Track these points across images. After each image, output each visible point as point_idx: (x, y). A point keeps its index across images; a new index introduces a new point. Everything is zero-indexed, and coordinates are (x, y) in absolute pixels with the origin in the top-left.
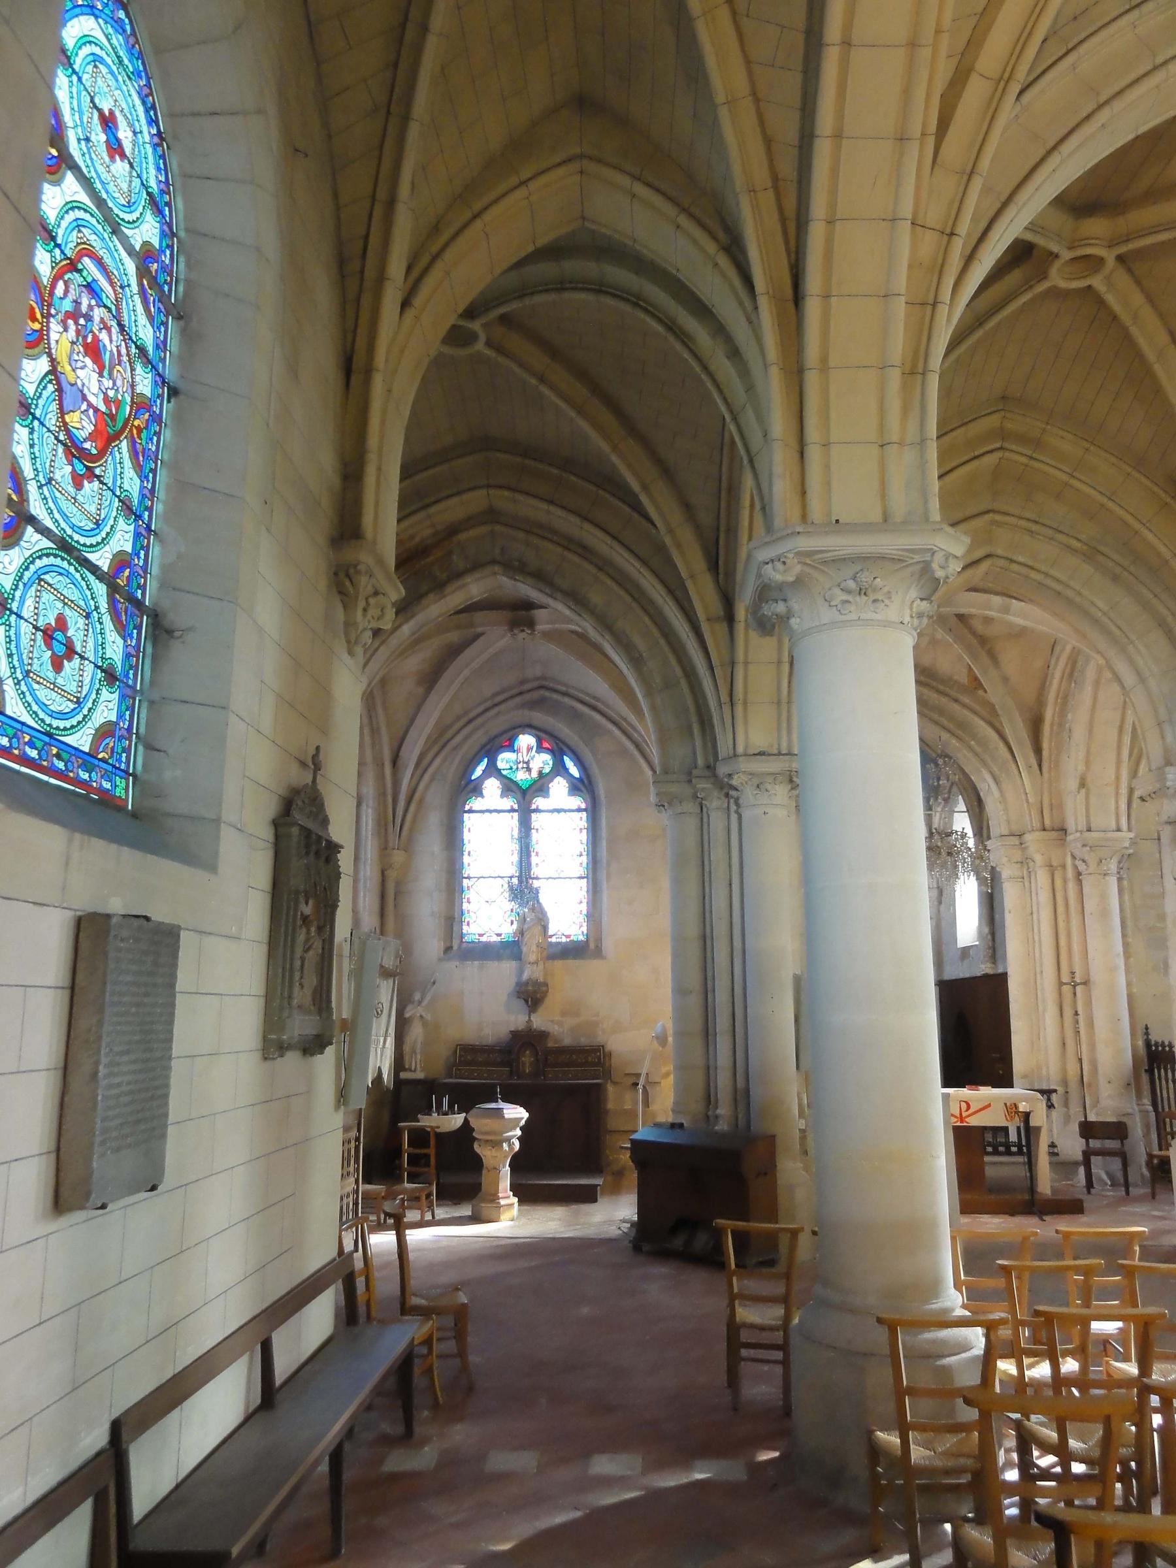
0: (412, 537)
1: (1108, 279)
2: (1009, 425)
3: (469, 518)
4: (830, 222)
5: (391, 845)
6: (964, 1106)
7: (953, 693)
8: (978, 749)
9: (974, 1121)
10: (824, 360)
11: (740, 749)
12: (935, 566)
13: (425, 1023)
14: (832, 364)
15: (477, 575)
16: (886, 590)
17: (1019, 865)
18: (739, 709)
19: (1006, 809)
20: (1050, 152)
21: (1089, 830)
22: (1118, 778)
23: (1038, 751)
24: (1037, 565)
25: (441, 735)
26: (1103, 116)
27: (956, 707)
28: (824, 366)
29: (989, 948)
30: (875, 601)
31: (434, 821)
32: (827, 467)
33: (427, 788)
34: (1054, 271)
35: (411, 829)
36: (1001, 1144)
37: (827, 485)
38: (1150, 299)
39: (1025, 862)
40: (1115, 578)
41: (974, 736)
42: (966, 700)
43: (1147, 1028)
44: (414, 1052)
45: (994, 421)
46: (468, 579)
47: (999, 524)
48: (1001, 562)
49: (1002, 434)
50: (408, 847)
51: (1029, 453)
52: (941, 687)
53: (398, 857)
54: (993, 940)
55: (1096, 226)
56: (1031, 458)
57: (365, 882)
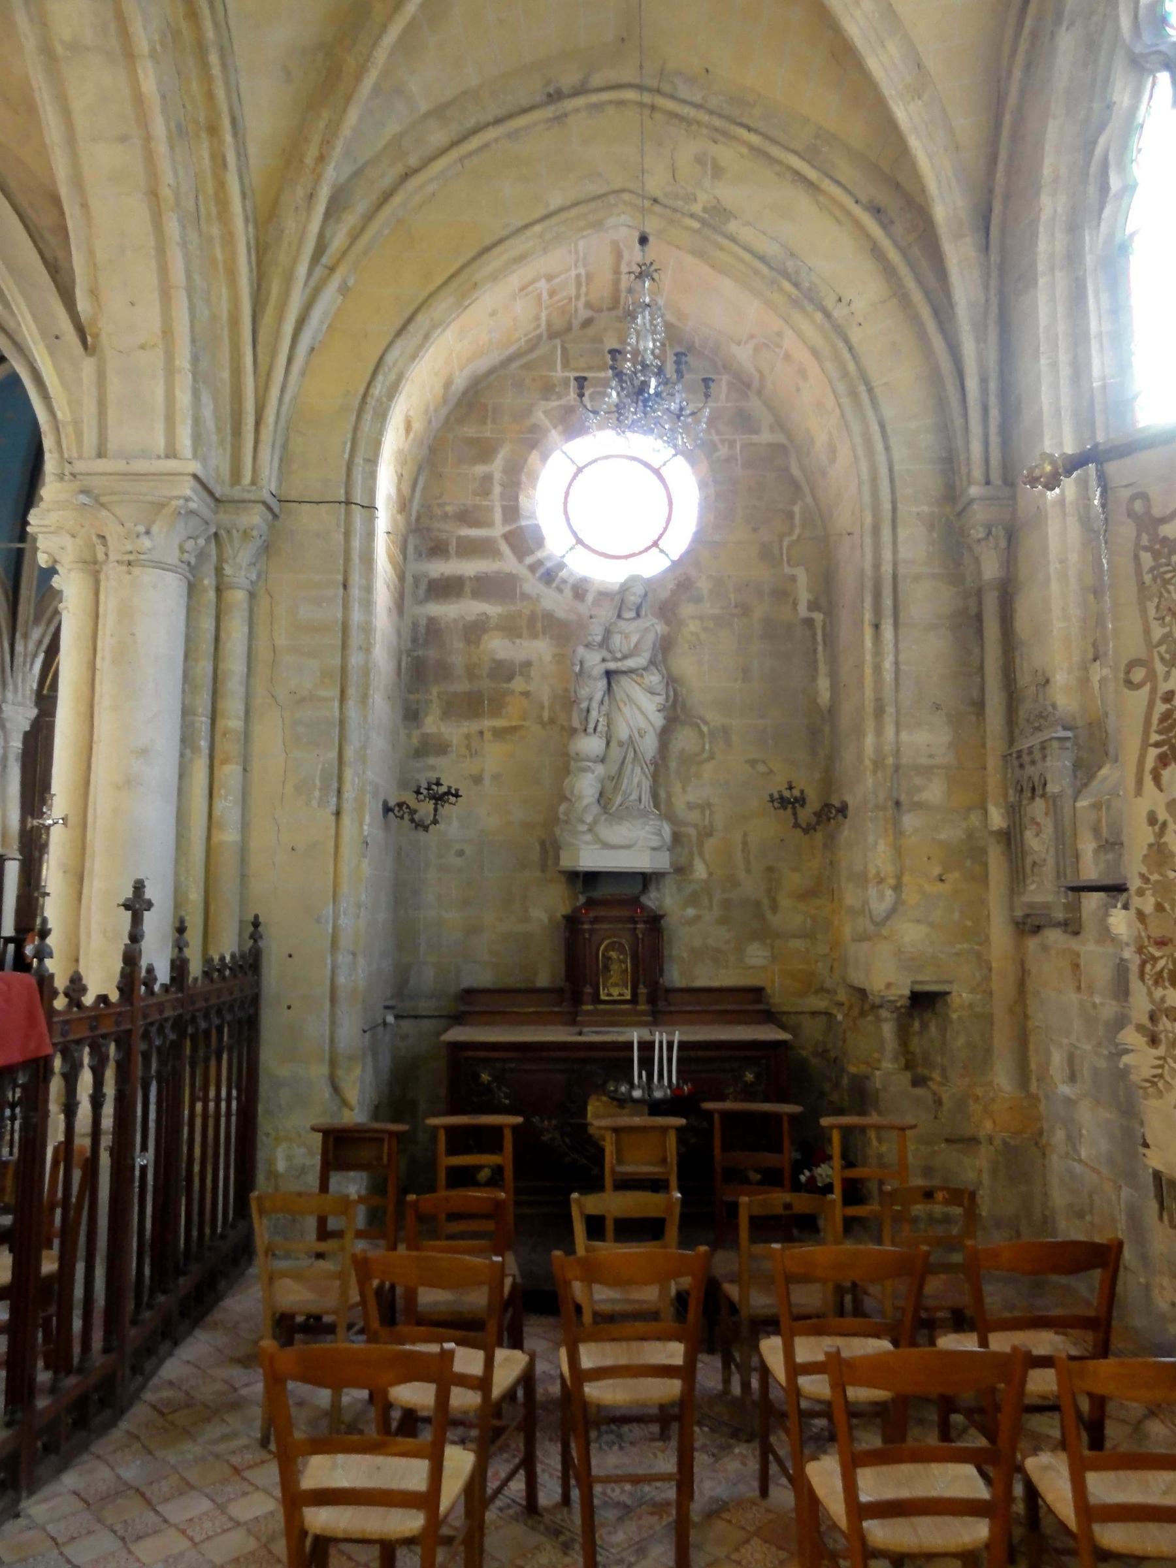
21: (101, 454)
22: (167, 332)
43: (256, 924)
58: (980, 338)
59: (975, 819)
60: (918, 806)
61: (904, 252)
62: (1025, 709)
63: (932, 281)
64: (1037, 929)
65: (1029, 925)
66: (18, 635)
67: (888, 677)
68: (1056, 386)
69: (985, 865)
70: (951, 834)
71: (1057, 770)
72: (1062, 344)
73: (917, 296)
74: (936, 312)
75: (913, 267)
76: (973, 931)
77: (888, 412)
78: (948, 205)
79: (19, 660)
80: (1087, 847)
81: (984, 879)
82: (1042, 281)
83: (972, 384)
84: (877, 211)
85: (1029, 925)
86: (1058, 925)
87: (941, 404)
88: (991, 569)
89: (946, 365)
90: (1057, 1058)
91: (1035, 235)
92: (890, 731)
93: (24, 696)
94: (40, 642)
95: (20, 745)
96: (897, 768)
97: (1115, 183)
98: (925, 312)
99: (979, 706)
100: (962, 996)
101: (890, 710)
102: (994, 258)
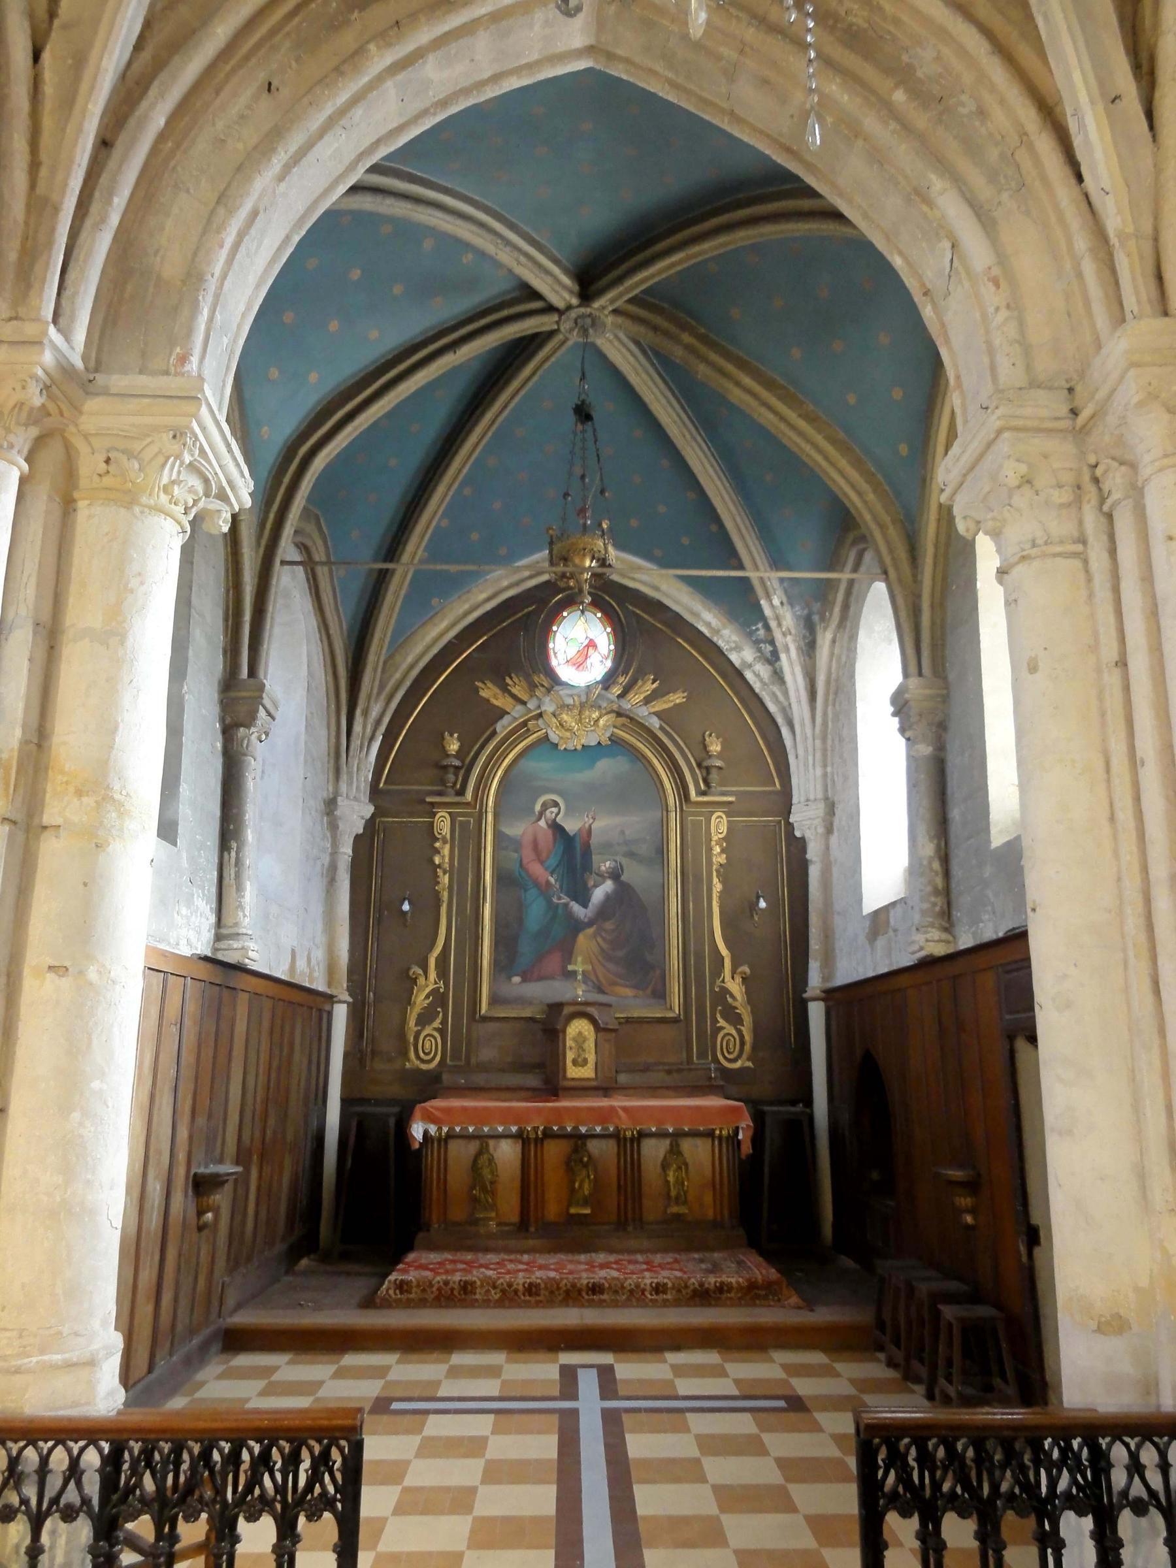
19: (1015, 306)
29: (936, 892)
41: (904, 76)
54: (947, 874)
66: (358, 712)
79: (356, 742)
93: (358, 788)
94: (378, 722)
95: (350, 852)
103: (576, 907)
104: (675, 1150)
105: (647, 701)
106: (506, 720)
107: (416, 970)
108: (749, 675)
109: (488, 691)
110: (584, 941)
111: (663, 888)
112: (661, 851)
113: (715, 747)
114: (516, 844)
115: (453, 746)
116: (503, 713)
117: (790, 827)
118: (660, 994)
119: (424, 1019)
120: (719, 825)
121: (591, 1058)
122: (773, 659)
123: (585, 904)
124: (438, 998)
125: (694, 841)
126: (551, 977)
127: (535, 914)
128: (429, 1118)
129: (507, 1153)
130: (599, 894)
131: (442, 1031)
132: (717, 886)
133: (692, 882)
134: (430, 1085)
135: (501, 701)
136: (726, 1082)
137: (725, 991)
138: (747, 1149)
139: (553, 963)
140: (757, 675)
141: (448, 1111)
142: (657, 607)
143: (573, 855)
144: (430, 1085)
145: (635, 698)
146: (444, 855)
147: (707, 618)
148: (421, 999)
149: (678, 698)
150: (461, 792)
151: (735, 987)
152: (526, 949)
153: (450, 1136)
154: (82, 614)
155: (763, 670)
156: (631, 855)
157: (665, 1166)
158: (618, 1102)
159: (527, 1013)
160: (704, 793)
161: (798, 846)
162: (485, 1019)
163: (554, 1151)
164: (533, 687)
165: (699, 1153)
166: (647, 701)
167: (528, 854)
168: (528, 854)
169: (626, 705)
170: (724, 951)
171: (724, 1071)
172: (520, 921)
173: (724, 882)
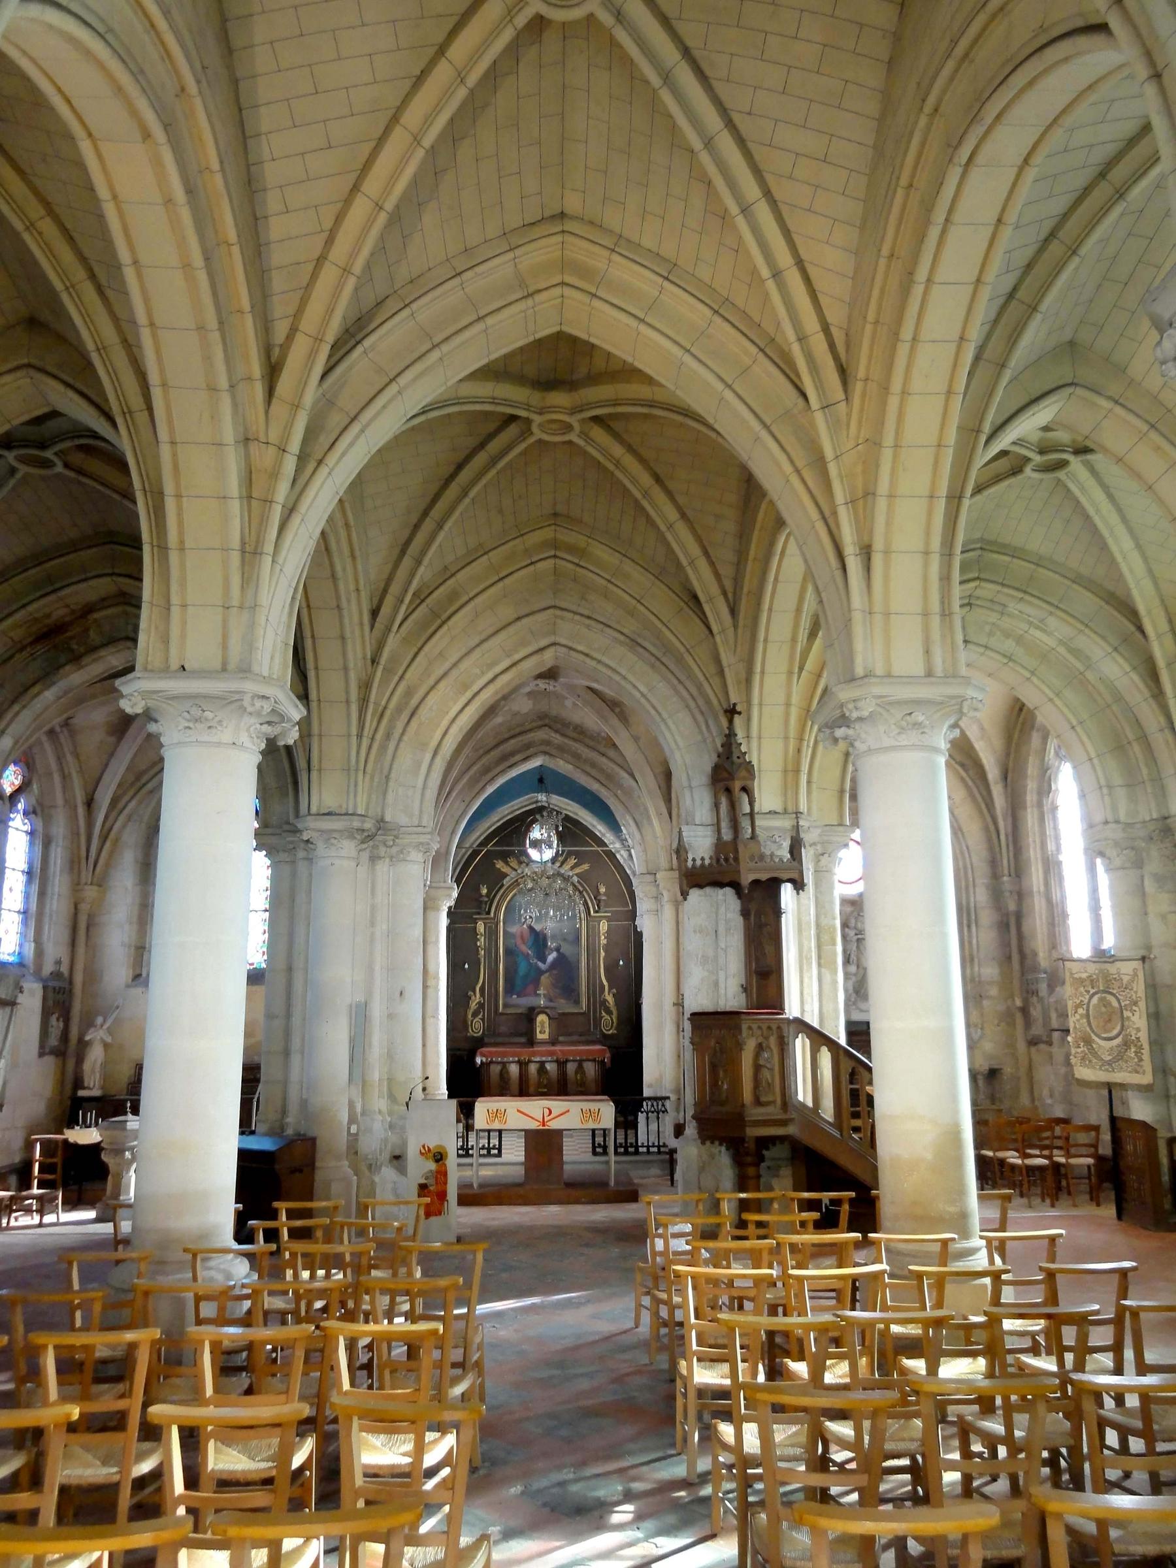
0: (48, 616)
1: (584, 435)
2: (560, 536)
3: (103, 600)
4: (173, 443)
5: (83, 881)
6: (547, 1112)
7: (602, 750)
8: (623, 799)
9: (554, 1125)
10: (182, 542)
11: (314, 810)
12: (246, 703)
13: (106, 1046)
14: (187, 545)
15: (111, 649)
16: (217, 719)
17: (652, 900)
18: (314, 774)
20: (391, 381)
23: (668, 800)
24: (595, 655)
25: (138, 778)
26: (436, 355)
27: (604, 760)
28: (182, 549)
30: (210, 727)
31: (128, 860)
32: (184, 623)
33: (124, 826)
34: (535, 429)
35: (108, 865)
36: (631, 1145)
37: (183, 636)
38: (630, 449)
39: (657, 898)
40: (653, 666)
41: (620, 786)
42: (612, 753)
44: (93, 1071)
45: (547, 534)
46: (103, 653)
47: (562, 618)
48: (564, 650)
49: (555, 544)
50: (101, 883)
51: (576, 561)
52: (592, 744)
53: (90, 892)
55: (559, 398)
56: (578, 565)
57: (51, 915)
58: (1005, 820)
59: (1009, 1002)
60: (989, 997)
61: (972, 780)
62: (1029, 962)
63: (985, 793)
64: (1036, 1044)
65: (1033, 1042)
67: (975, 946)
68: (1035, 849)
69: (1014, 1020)
70: (1001, 1007)
71: (1043, 988)
72: (1037, 835)
73: (980, 799)
74: (987, 805)
75: (977, 787)
76: (1011, 1045)
77: (970, 843)
78: (993, 773)
80: (1054, 1015)
81: (1014, 1025)
82: (1029, 810)
83: (1003, 837)
84: (962, 765)
85: (1033, 1042)
86: (1043, 1042)
87: (989, 840)
88: (1012, 906)
89: (992, 828)
90: (1046, 1092)
91: (1025, 793)
92: (976, 969)
96: (980, 982)
97: (1053, 788)
98: (983, 806)
99: (1009, 958)
100: (1008, 1070)
101: (976, 960)
102: (1009, 789)
103: (540, 964)
104: (580, 1068)
105: (572, 868)
106: (508, 878)
107: (470, 993)
108: (618, 856)
109: (500, 865)
110: (544, 979)
111: (579, 954)
112: (578, 939)
113: (603, 890)
114: (513, 936)
115: (484, 891)
116: (505, 875)
117: (635, 927)
118: (577, 1002)
119: (475, 1015)
120: (604, 926)
121: (547, 1030)
122: (629, 851)
123: (544, 962)
124: (481, 1006)
125: (592, 933)
126: (529, 995)
127: (522, 969)
128: (483, 1055)
129: (514, 1069)
130: (551, 957)
131: (483, 1020)
132: (603, 954)
133: (592, 953)
134: (478, 1043)
135: (505, 869)
136: (605, 1039)
137: (605, 1000)
138: (608, 1065)
139: (530, 988)
140: (622, 856)
141: (490, 1052)
142: (577, 823)
143: (539, 940)
144: (478, 1043)
145: (567, 867)
146: (481, 942)
147: (600, 828)
148: (473, 1005)
149: (586, 867)
150: (488, 913)
151: (610, 999)
152: (518, 982)
153: (491, 1062)
154: (431, 939)
155: (625, 854)
156: (565, 940)
157: (576, 1073)
158: (558, 1048)
159: (519, 1011)
160: (596, 912)
161: (639, 935)
162: (502, 1014)
163: (533, 1068)
164: (520, 863)
165: (590, 1069)
166: (572, 868)
167: (519, 941)
168: (519, 941)
169: (562, 871)
170: (605, 983)
171: (604, 1036)
172: (516, 971)
173: (606, 951)
